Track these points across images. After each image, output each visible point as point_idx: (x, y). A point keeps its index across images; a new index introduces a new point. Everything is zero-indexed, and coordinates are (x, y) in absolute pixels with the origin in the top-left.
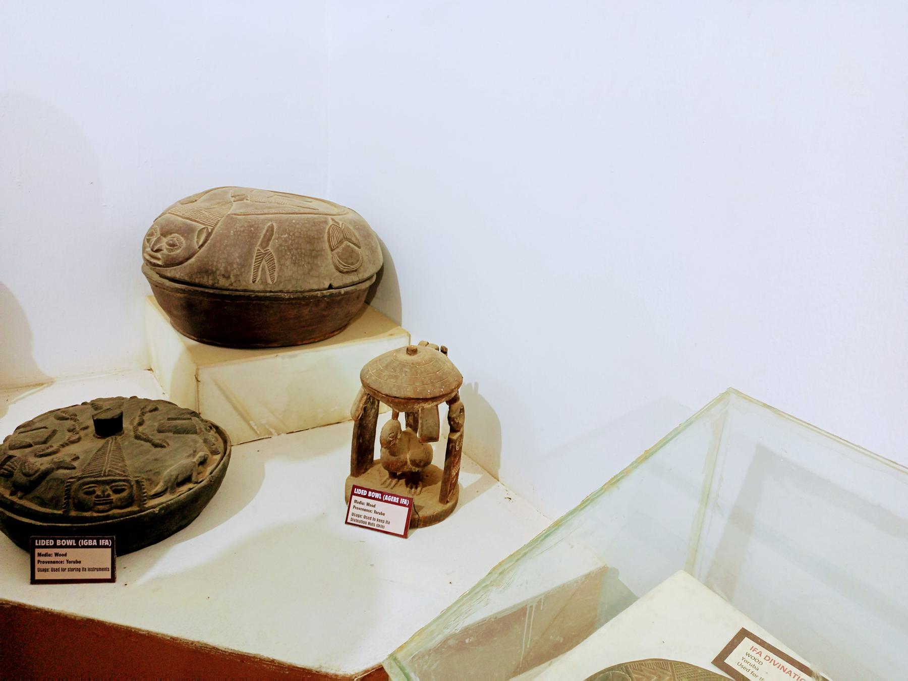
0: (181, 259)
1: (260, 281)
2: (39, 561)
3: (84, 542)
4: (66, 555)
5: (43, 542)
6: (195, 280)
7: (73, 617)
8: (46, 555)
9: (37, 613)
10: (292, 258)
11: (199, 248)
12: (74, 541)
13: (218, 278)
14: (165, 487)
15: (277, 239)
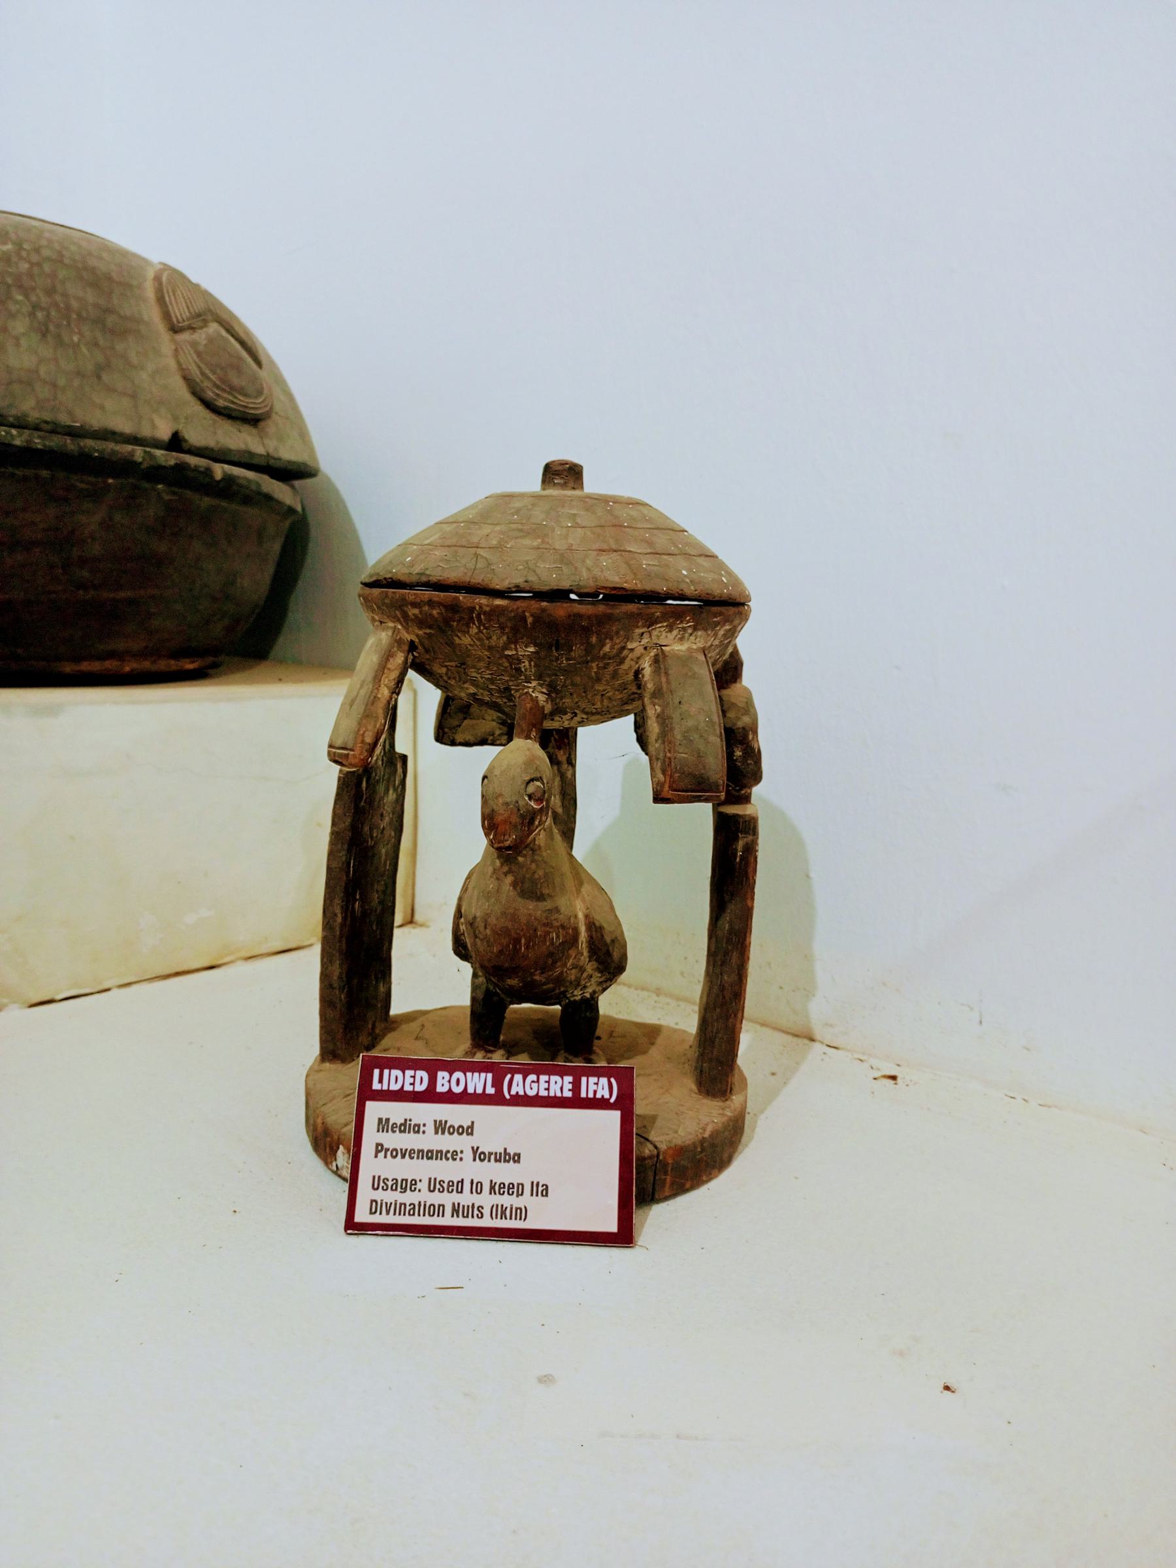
2: (379, 1148)
4: (469, 1130)
5: (394, 1079)
8: (405, 1127)
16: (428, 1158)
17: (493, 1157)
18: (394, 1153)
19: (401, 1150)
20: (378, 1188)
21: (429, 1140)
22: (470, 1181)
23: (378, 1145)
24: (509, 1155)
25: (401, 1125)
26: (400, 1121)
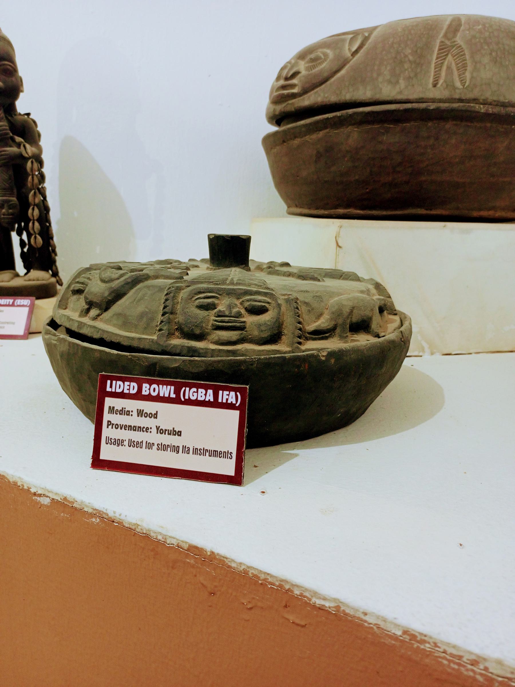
0: (326, 74)
1: (445, 85)
2: (109, 423)
3: (191, 393)
5: (118, 386)
6: (345, 96)
7: (160, 537)
8: (123, 412)
9: (94, 520)
10: (491, 54)
11: (352, 55)
12: (173, 388)
13: (380, 86)
14: (333, 323)
15: (469, 30)
16: (134, 430)
17: (167, 432)
18: (117, 426)
19: (120, 425)
20: (108, 444)
21: (134, 420)
22: (145, 442)
23: (109, 421)
24: (175, 431)
25: (120, 410)
26: (120, 408)
